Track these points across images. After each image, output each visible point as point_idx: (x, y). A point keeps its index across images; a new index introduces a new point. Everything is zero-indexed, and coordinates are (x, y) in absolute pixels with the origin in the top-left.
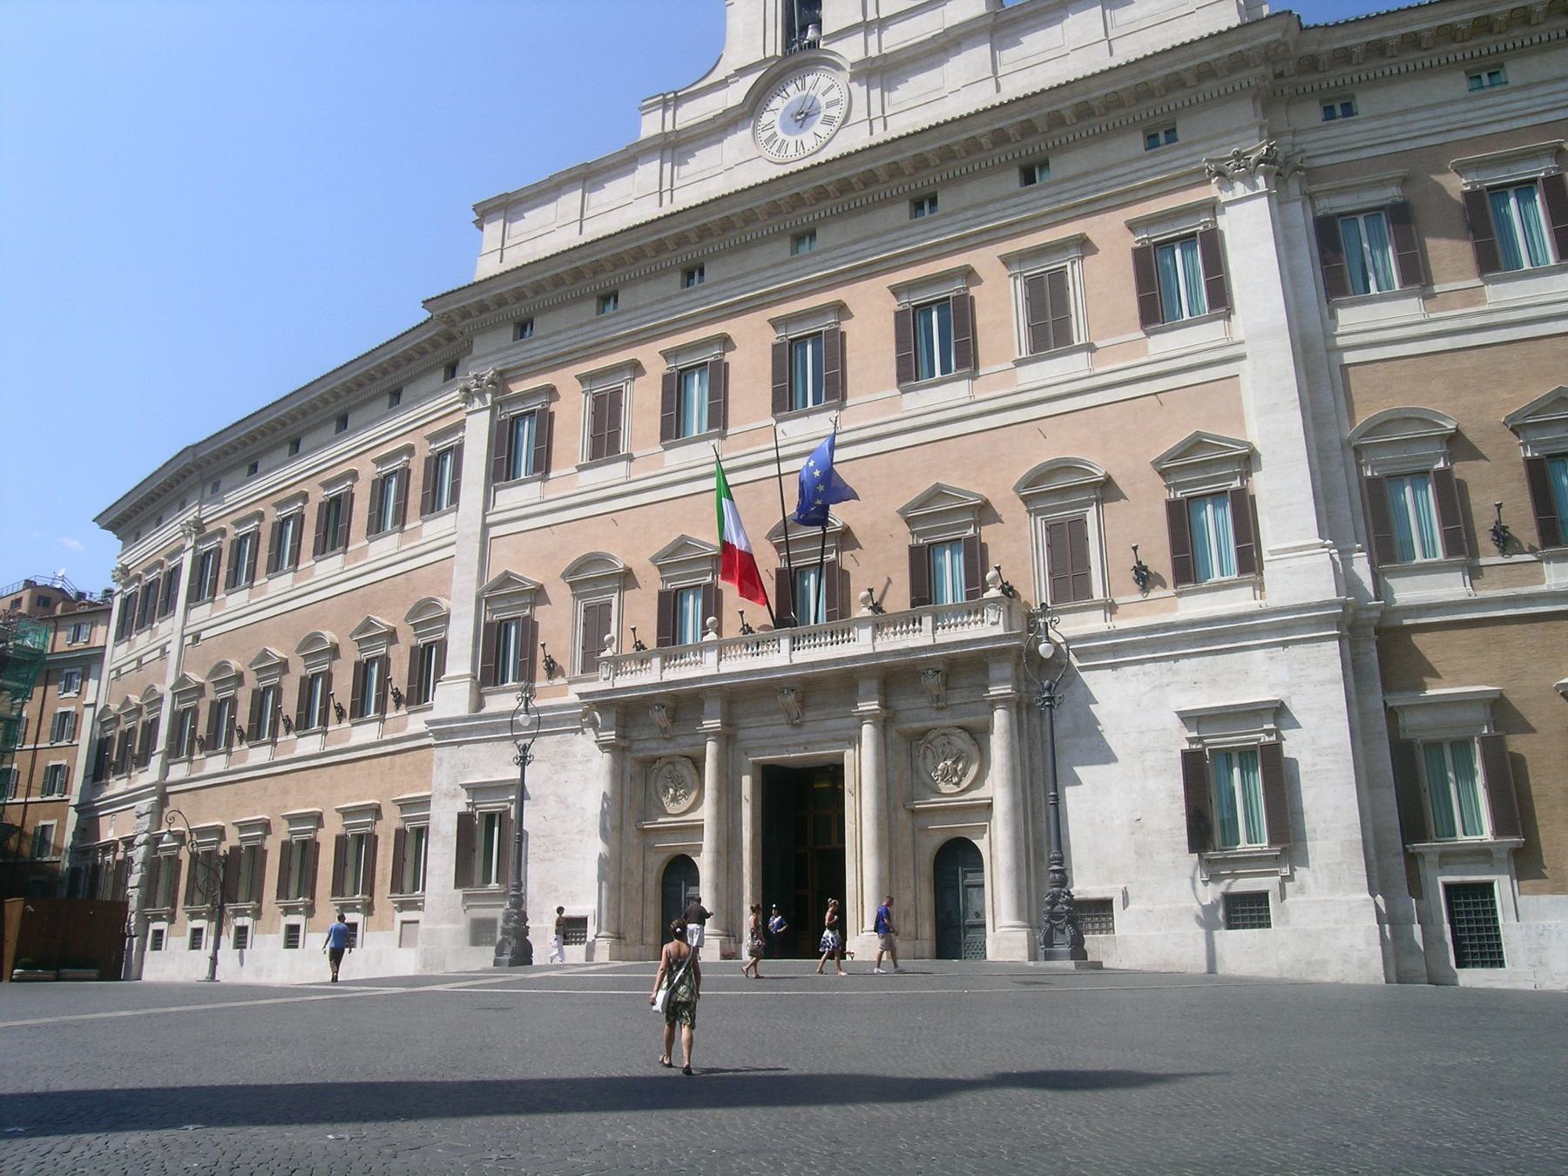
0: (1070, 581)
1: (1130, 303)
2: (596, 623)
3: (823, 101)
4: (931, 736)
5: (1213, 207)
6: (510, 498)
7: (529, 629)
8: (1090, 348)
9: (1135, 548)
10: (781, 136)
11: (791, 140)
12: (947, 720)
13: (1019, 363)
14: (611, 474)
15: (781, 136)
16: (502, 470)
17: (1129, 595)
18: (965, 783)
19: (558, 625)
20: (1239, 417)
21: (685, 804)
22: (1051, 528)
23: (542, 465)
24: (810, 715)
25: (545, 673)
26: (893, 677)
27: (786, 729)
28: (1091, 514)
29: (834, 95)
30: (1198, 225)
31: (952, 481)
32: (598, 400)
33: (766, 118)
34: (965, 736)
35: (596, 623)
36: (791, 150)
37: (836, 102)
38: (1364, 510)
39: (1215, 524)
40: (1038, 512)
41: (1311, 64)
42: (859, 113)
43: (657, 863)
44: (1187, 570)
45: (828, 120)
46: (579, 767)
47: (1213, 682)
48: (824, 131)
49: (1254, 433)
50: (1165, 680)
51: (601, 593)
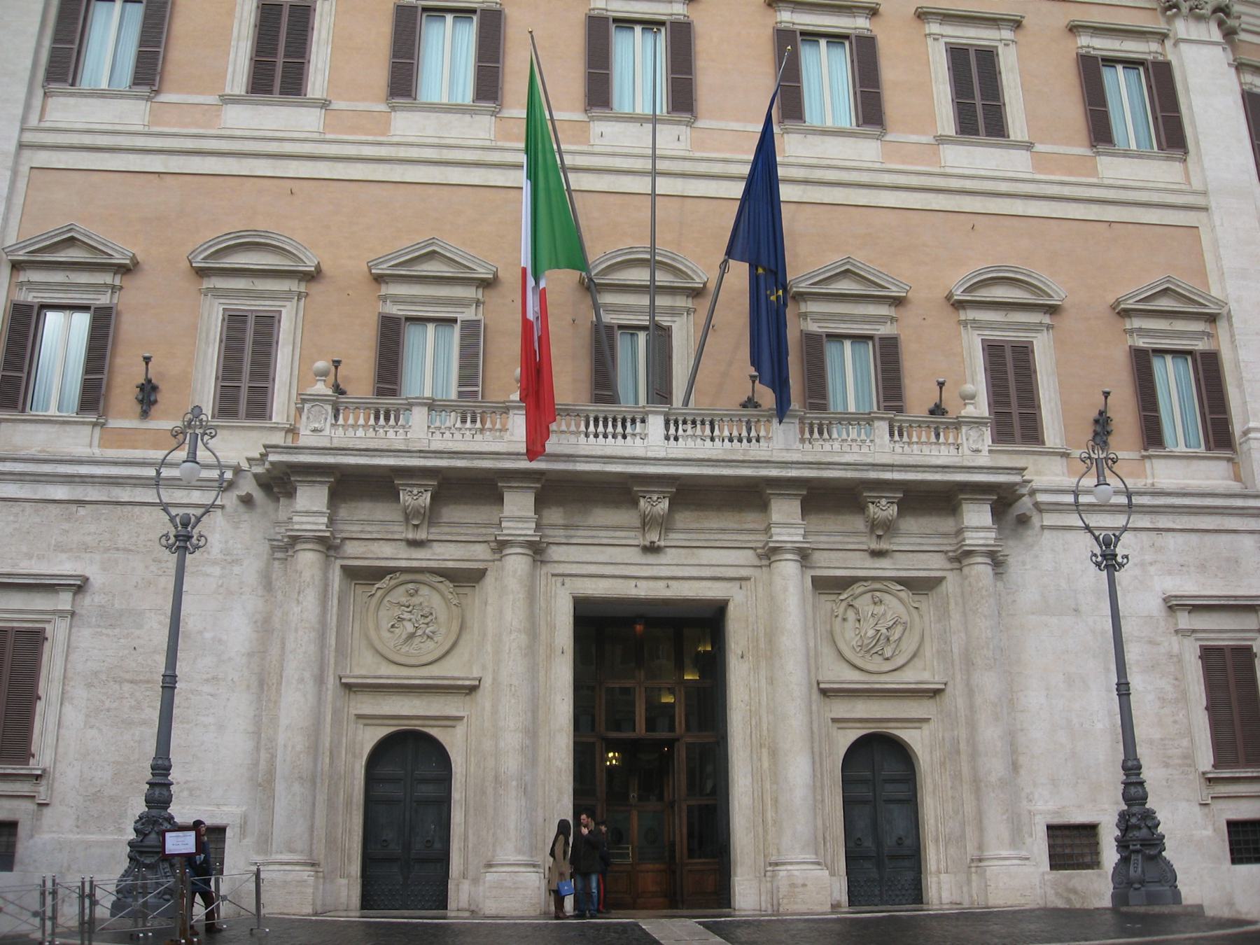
0: (1015, 414)
1: (1073, 110)
4: (858, 589)
5: (1163, 37)
6: (68, 112)
8: (1028, 146)
9: (1106, 394)
12: (885, 568)
13: (941, 140)
18: (900, 661)
20: (1202, 273)
21: (430, 649)
22: (993, 351)
24: (675, 538)
25: (138, 408)
26: (828, 497)
27: (633, 555)
31: (863, 258)
34: (905, 594)
39: (1173, 382)
40: (977, 325)
43: (371, 737)
46: (217, 571)
47: (1202, 567)
50: (1148, 557)
51: (260, 295)
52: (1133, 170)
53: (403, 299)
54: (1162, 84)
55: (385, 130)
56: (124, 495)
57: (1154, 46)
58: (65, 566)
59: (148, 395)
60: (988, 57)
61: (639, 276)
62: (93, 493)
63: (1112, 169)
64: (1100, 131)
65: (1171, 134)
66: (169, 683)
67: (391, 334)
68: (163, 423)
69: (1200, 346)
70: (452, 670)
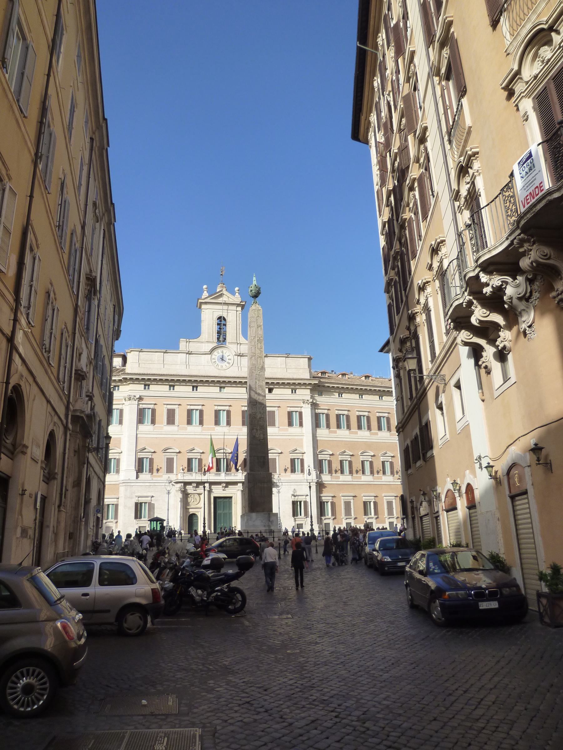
1: (286, 421)
2: (170, 462)
3: (228, 358)
6: (141, 427)
7: (151, 461)
10: (217, 362)
11: (220, 364)
14: (171, 428)
15: (217, 362)
16: (140, 420)
17: (283, 474)
19: (160, 461)
20: (302, 446)
23: (153, 422)
28: (277, 458)
29: (229, 357)
30: (298, 409)
32: (168, 410)
33: (213, 356)
35: (170, 462)
36: (220, 367)
37: (230, 359)
38: (319, 465)
41: (319, 386)
42: (235, 364)
44: (293, 471)
45: (229, 363)
48: (227, 365)
49: (305, 450)
52: (295, 429)
53: (191, 455)
54: (301, 414)
55: (186, 430)
56: (156, 484)
57: (299, 409)
58: (150, 494)
59: (158, 470)
60: (274, 412)
61: (222, 451)
62: (152, 484)
63: (291, 430)
64: (290, 424)
65: (301, 424)
66: (168, 510)
67: (190, 461)
68: (159, 474)
69: (301, 457)
70: (198, 506)
